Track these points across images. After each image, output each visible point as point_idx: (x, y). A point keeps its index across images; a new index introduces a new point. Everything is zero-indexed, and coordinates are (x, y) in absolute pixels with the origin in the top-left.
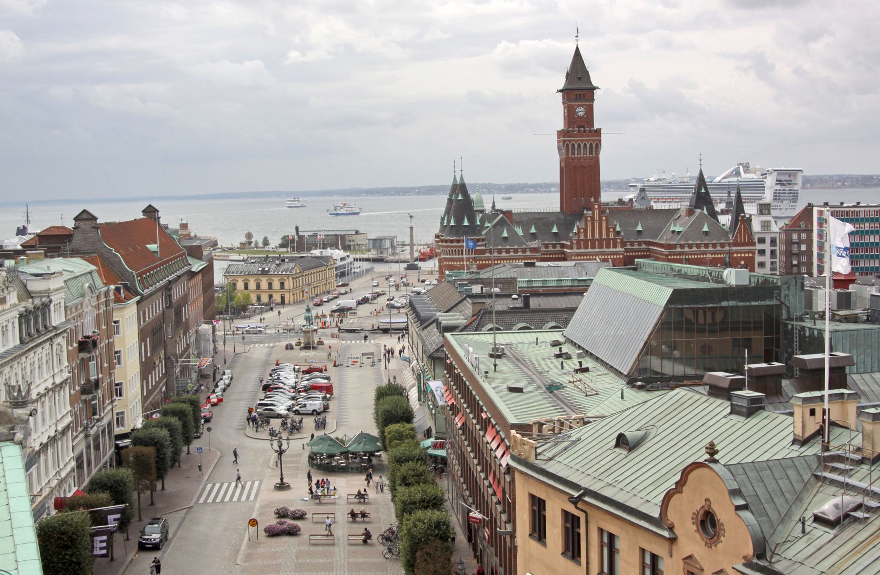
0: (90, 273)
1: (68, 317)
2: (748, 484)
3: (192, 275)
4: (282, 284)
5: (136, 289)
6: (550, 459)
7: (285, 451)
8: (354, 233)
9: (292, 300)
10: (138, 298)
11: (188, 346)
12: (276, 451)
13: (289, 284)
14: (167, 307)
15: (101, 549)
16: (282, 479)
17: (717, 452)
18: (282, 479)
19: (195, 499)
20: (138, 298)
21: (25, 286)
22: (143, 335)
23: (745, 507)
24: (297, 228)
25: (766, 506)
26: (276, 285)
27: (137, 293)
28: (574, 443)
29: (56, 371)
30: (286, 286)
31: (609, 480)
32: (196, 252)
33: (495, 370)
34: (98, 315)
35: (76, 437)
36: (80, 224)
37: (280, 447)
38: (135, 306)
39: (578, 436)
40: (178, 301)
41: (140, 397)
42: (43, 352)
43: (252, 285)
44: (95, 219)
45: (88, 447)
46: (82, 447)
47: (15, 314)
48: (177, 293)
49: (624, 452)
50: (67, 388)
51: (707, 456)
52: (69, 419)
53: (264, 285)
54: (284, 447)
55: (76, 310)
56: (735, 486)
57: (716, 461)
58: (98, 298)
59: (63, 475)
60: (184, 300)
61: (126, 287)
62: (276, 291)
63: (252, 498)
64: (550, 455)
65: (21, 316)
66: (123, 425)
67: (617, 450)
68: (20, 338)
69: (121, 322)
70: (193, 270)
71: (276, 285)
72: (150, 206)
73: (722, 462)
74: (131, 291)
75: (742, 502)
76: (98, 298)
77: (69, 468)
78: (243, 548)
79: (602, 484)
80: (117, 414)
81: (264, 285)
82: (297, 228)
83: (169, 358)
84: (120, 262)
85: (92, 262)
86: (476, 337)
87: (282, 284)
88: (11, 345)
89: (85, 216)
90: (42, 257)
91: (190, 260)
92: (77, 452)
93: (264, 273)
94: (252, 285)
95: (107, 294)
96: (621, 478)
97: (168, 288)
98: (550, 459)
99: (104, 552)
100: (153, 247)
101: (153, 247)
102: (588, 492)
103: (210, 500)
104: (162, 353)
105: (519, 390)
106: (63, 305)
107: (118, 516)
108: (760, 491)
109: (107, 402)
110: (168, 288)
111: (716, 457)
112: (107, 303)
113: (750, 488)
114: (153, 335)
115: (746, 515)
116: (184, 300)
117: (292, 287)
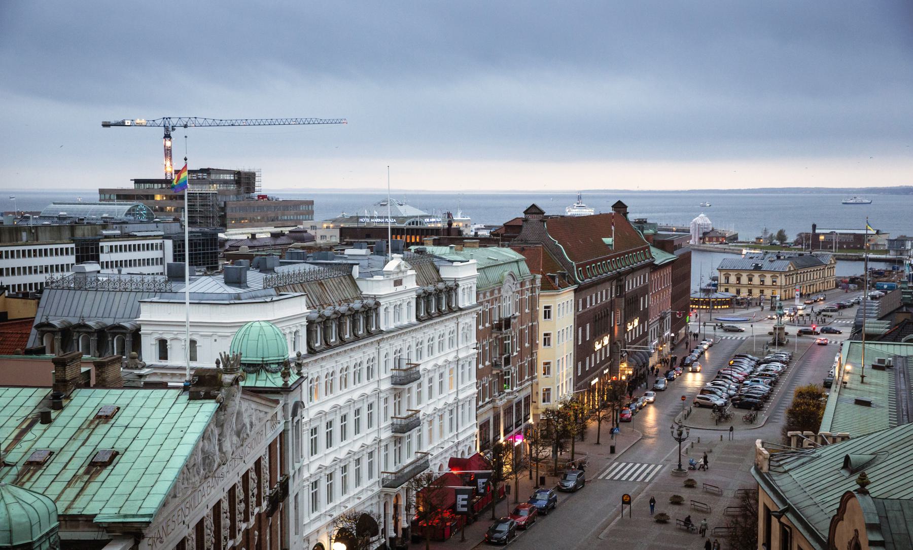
0: (517, 262)
1: (480, 300)
2: (901, 521)
3: (654, 268)
6: (786, 472)
7: (684, 440)
8: (875, 232)
10: (575, 286)
11: (645, 334)
12: (676, 439)
14: (616, 297)
15: (463, 506)
16: (680, 466)
17: (868, 483)
18: (680, 466)
19: (596, 475)
20: (575, 286)
22: (580, 321)
24: (814, 227)
26: (768, 280)
27: (575, 282)
28: (814, 458)
29: (461, 346)
31: (818, 499)
32: (665, 245)
33: (862, 382)
34: (521, 300)
35: (482, 406)
36: (530, 217)
37: (680, 434)
38: (572, 294)
39: (819, 453)
40: (634, 291)
41: (572, 376)
42: (444, 327)
43: (744, 280)
44: (542, 213)
45: (497, 418)
46: (490, 416)
47: (414, 295)
48: (632, 284)
49: (847, 474)
51: (858, 487)
53: (756, 280)
54: (683, 437)
55: (492, 293)
56: (876, 520)
57: (866, 493)
58: (522, 284)
59: (461, 438)
60: (644, 291)
61: (563, 276)
62: (768, 287)
63: (647, 480)
64: (787, 468)
65: (418, 298)
66: (549, 401)
67: (843, 472)
70: (656, 263)
71: (768, 280)
72: (619, 202)
73: (873, 495)
74: (566, 280)
75: (877, 537)
76: (522, 284)
78: (613, 524)
79: (810, 502)
82: (814, 227)
83: (615, 343)
85: (521, 251)
86: (878, 347)
88: (405, 323)
89: (534, 211)
90: (477, 245)
91: (655, 252)
92: (483, 419)
93: (757, 268)
95: (533, 281)
96: (829, 499)
97: (619, 278)
98: (786, 472)
99: (465, 509)
100: (608, 241)
101: (608, 241)
102: (789, 509)
103: (624, 479)
105: (868, 404)
106: (474, 289)
109: (526, 378)
110: (619, 278)
111: (867, 487)
112: (533, 290)
113: (903, 526)
114: (591, 322)
116: (644, 291)
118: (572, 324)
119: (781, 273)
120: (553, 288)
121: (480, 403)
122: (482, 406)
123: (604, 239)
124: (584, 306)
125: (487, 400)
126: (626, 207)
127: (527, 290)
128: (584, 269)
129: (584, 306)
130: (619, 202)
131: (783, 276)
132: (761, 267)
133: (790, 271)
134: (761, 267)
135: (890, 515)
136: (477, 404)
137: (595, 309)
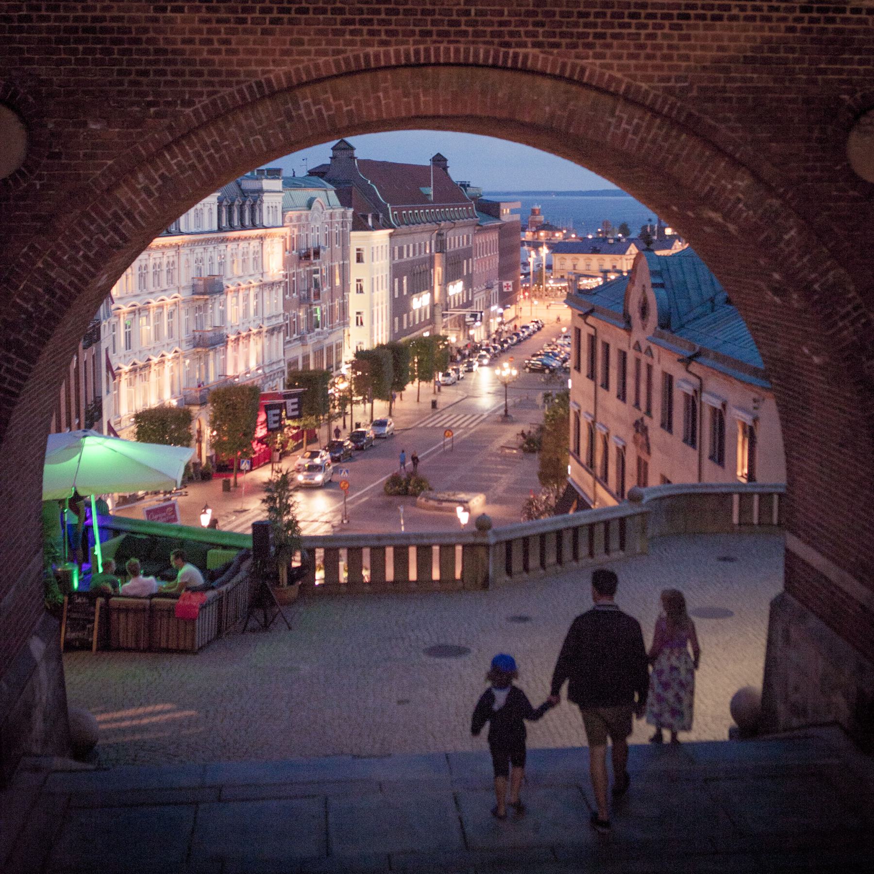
10: (391, 231)
21: (240, 186)
22: (397, 271)
23: (662, 286)
25: (691, 292)
35: (289, 342)
36: (338, 153)
50: (281, 291)
52: (281, 320)
61: (376, 218)
68: (219, 227)
72: (439, 155)
77: (275, 367)
84: (375, 193)
92: (290, 355)
107: (296, 400)
108: (690, 279)
115: (662, 292)
118: (388, 273)
120: (366, 228)
121: (288, 338)
122: (289, 342)
124: (401, 255)
125: (295, 336)
126: (446, 160)
127: (338, 222)
128: (400, 213)
129: (401, 255)
130: (439, 155)
135: (671, 268)
136: (284, 339)
137: (412, 262)
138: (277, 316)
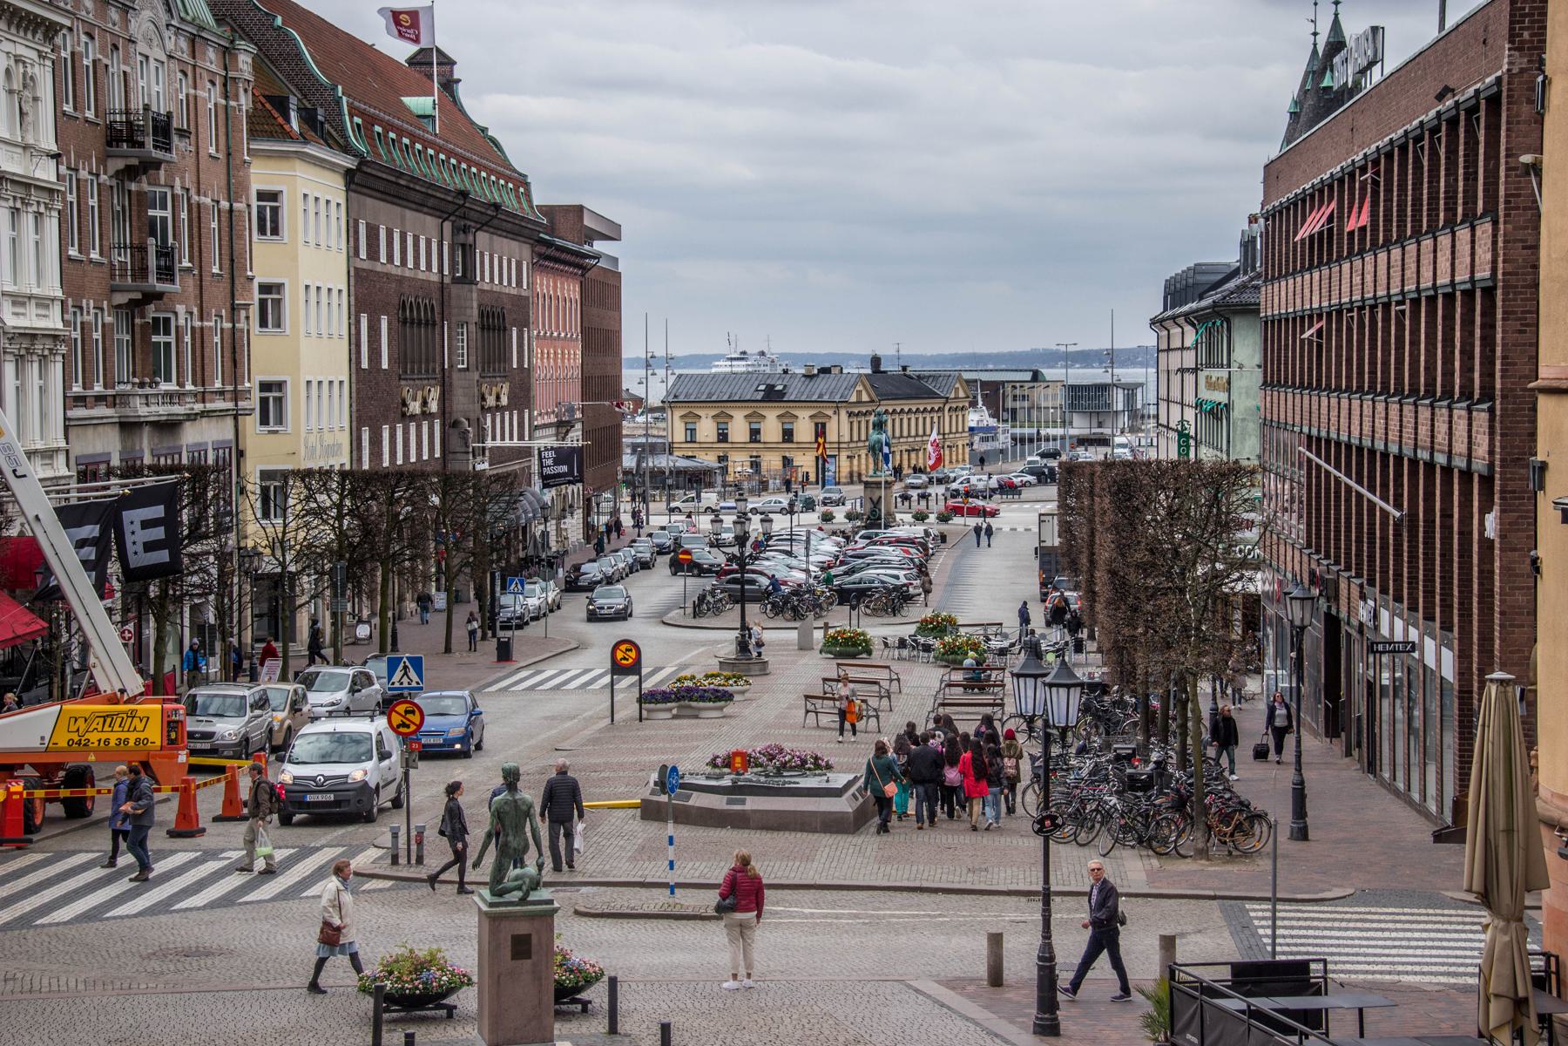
4: (820, 431)
5: (346, 137)
8: (1028, 376)
9: (845, 471)
13: (840, 426)
14: (455, 280)
20: (349, 162)
30: (832, 436)
43: (739, 429)
53: (771, 429)
61: (308, 117)
62: (802, 448)
69: (285, 198)
71: (804, 430)
80: (266, 475)
81: (771, 429)
83: (456, 424)
87: (820, 431)
94: (739, 429)
104: (434, 394)
117: (847, 439)
119: (837, 406)
123: (406, 100)
124: (373, 254)
131: (843, 413)
132: (782, 394)
133: (859, 402)
134: (782, 394)
137: (401, 280)
138: (43, 302)
